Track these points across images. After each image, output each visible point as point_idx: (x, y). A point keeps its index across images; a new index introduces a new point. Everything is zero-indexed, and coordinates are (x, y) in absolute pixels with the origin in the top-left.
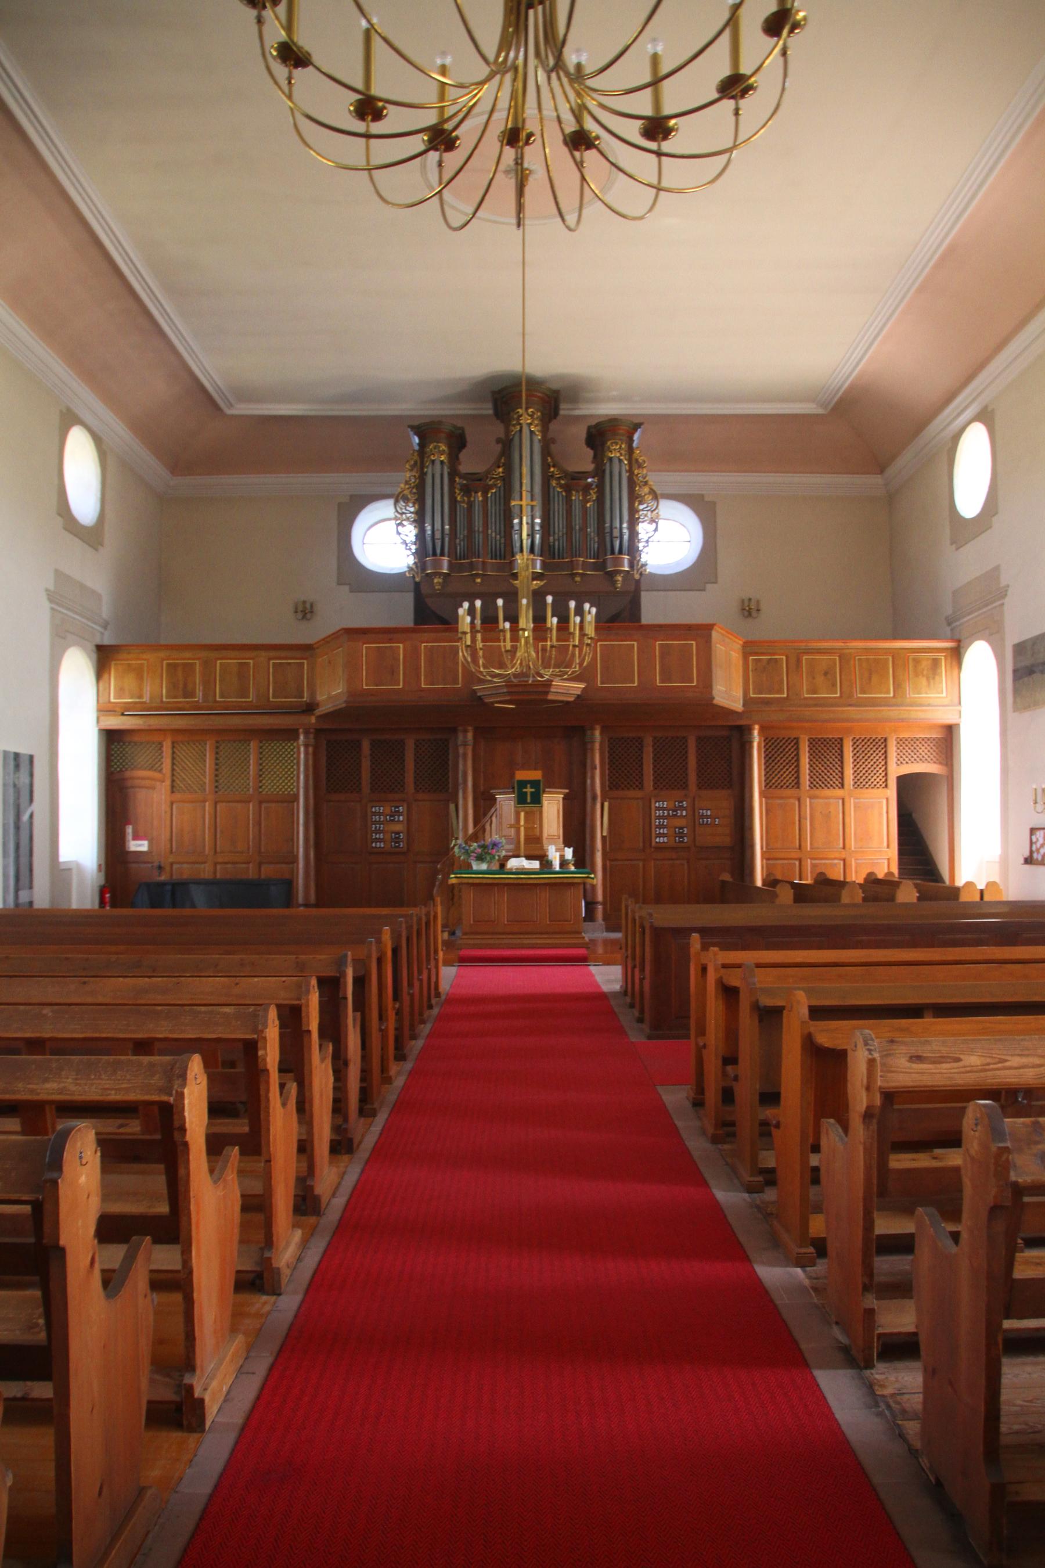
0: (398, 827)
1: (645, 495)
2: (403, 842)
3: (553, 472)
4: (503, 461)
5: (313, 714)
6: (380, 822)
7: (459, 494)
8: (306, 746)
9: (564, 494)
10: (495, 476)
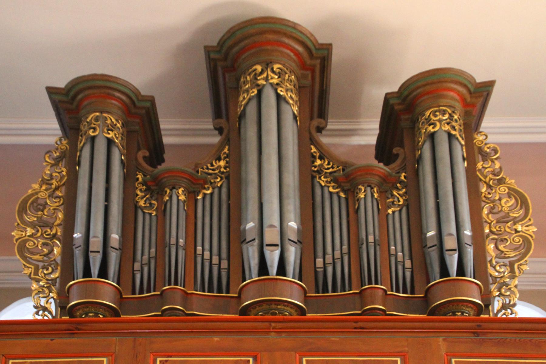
1: (500, 199)
4: (226, 150)
7: (142, 198)
9: (342, 195)
10: (211, 171)
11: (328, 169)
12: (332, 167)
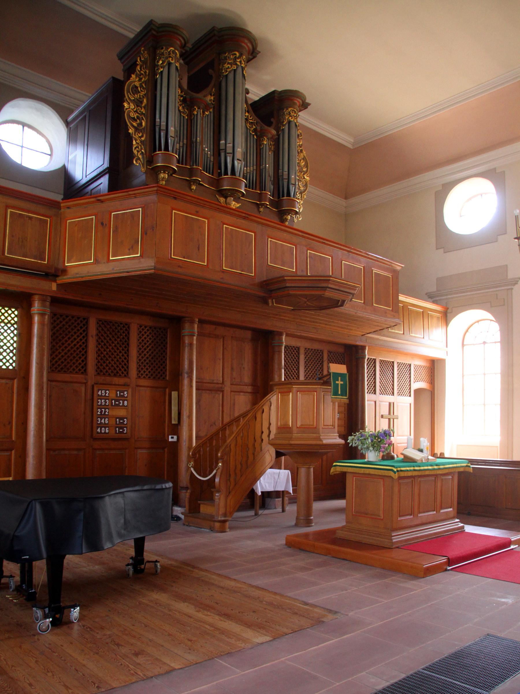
0: (122, 413)
2: (126, 427)
3: (248, 116)
5: (55, 281)
6: (106, 407)
8: (42, 315)
9: (255, 137)
11: (250, 120)
12: (252, 120)
